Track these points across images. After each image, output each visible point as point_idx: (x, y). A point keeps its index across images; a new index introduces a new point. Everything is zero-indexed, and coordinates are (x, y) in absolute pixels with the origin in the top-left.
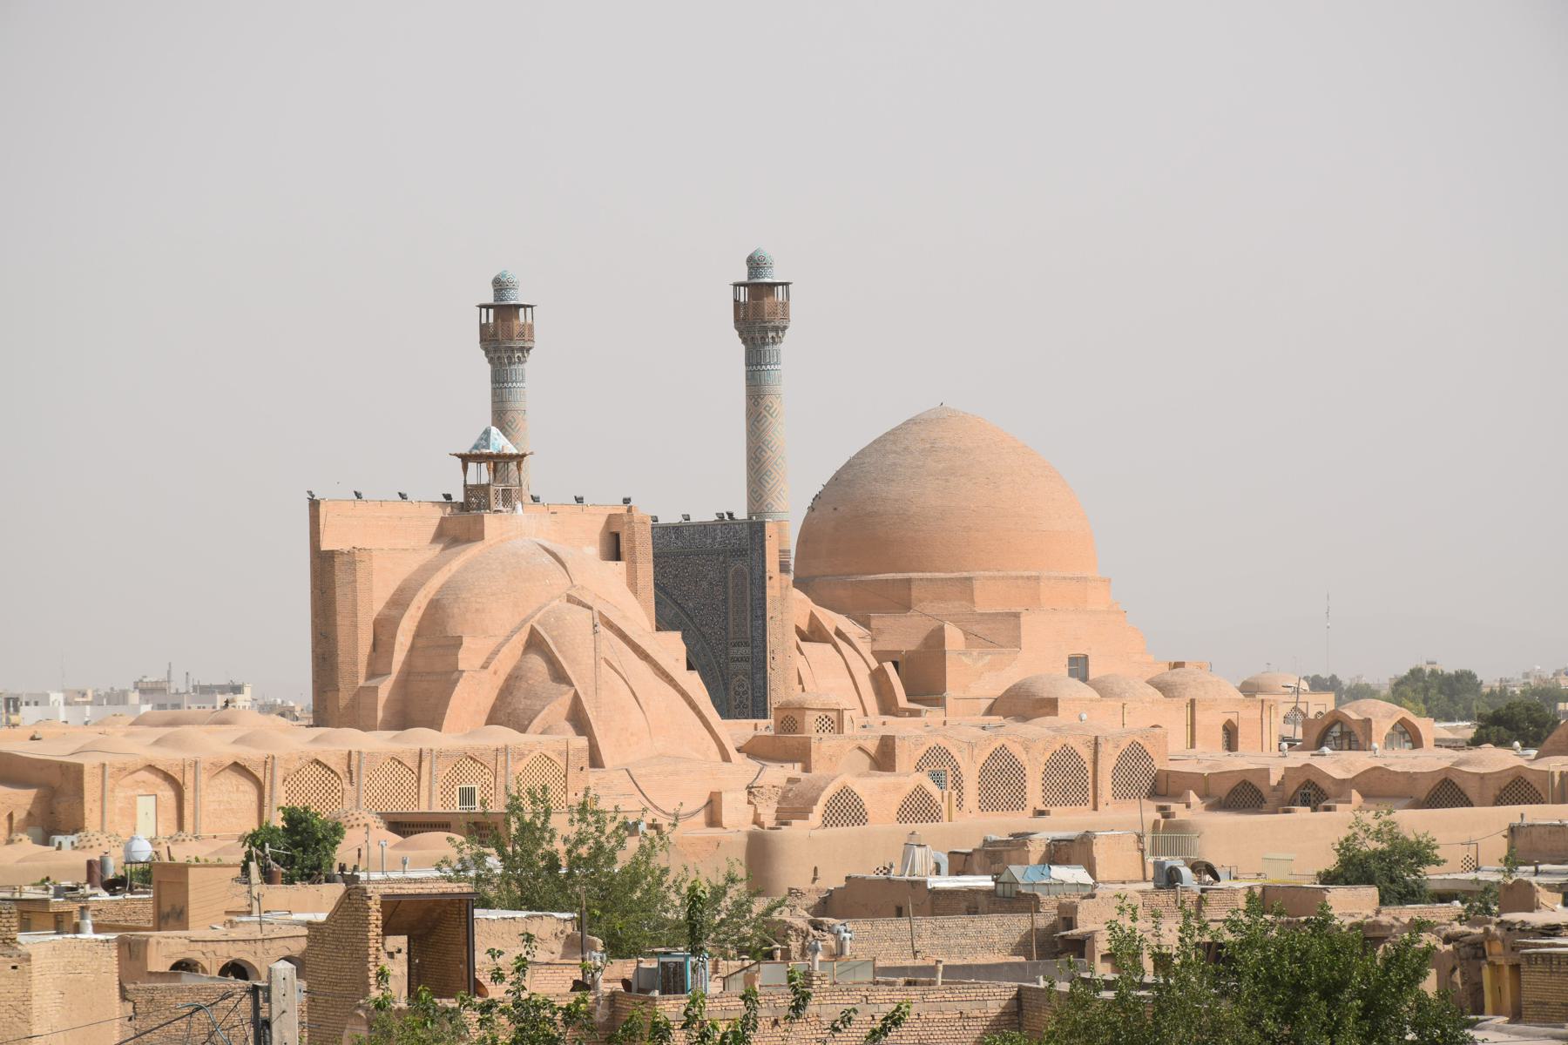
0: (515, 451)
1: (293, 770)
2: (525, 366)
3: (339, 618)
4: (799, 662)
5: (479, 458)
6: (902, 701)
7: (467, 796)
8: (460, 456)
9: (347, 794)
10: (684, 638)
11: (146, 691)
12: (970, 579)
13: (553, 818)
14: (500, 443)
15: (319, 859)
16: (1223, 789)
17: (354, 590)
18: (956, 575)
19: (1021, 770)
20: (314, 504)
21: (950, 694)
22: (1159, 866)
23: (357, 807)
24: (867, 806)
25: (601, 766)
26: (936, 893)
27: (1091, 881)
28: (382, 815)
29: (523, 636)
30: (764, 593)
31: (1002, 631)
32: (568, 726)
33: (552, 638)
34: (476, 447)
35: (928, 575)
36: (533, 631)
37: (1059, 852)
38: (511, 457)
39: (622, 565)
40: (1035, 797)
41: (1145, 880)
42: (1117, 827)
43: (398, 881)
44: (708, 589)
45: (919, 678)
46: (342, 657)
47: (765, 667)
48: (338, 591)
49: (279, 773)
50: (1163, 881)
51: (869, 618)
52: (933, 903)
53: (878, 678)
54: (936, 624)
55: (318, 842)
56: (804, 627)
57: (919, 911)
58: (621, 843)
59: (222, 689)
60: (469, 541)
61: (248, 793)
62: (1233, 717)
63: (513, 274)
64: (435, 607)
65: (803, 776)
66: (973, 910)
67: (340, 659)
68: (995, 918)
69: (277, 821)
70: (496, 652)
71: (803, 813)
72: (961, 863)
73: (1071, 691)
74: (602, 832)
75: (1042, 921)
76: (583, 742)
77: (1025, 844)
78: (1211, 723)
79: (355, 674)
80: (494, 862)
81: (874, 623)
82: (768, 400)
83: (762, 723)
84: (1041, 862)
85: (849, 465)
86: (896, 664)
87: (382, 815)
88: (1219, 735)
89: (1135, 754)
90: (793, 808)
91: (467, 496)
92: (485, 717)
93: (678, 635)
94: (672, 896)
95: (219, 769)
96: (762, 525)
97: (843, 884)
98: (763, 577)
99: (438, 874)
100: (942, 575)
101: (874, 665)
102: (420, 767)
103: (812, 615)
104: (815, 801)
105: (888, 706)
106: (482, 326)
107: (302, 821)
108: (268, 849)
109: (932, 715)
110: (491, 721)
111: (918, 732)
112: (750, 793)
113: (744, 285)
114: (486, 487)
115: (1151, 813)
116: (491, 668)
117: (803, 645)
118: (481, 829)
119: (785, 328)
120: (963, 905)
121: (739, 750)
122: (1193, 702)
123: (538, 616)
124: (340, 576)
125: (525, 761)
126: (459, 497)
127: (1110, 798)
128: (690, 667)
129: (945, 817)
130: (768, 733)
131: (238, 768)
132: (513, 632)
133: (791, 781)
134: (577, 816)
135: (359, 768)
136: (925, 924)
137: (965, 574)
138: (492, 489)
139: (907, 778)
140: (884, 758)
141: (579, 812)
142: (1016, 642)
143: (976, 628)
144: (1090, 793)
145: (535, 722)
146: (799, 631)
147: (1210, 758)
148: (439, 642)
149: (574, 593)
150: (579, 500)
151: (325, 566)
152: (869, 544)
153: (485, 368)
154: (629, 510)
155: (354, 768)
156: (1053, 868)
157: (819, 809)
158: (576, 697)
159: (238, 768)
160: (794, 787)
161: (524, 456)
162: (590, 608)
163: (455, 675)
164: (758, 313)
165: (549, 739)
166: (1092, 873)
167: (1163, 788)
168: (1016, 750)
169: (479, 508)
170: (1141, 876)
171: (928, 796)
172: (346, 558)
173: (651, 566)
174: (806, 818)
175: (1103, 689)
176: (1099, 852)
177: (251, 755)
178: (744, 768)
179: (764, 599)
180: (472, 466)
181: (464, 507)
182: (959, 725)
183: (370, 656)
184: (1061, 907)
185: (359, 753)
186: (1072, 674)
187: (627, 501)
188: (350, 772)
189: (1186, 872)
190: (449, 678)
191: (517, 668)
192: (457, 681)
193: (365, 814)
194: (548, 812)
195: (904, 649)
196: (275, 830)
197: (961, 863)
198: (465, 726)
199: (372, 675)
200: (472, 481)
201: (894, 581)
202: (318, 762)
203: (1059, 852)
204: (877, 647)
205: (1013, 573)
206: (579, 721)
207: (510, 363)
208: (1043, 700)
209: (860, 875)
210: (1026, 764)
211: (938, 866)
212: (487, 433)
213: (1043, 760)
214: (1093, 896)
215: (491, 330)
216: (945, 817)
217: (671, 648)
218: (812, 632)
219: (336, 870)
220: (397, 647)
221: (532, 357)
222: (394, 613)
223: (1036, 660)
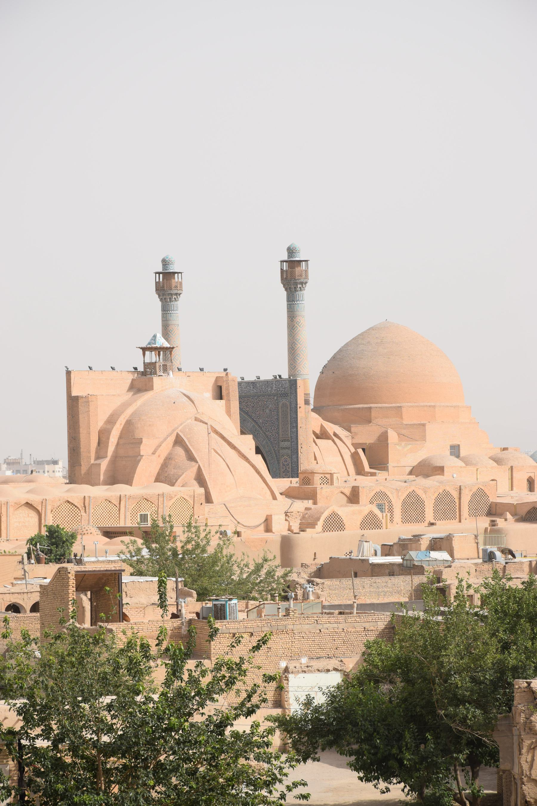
0: (168, 346)
1: (56, 506)
2: (178, 302)
3: (81, 430)
4: (315, 449)
5: (151, 349)
6: (367, 468)
7: (144, 518)
8: (141, 348)
9: (83, 517)
10: (253, 438)
11: (10, 463)
12: (400, 407)
13: (174, 530)
14: (161, 342)
15: (65, 552)
16: (523, 511)
17: (89, 416)
18: (394, 405)
19: (422, 502)
20: (68, 373)
21: (391, 465)
22: (485, 551)
23: (89, 524)
24: (344, 522)
25: (212, 502)
26: (374, 565)
27: (450, 559)
28: (99, 528)
29: (172, 438)
30: (297, 415)
31: (417, 433)
32: (195, 483)
33: (188, 439)
34: (149, 344)
35: (380, 405)
36: (178, 436)
37: (436, 545)
38: (167, 348)
39: (223, 402)
40: (429, 516)
41: (478, 557)
42: (467, 531)
43: (103, 562)
44: (268, 415)
45: (375, 457)
46: (83, 449)
47: (297, 452)
48: (81, 416)
49: (49, 508)
50: (487, 559)
51: (350, 427)
52: (372, 570)
53: (355, 457)
54: (383, 430)
55: (64, 542)
56: (318, 432)
57: (365, 574)
58: (208, 542)
59: (48, 462)
60: (146, 390)
61: (33, 517)
62: (532, 475)
63: (172, 256)
64: (129, 423)
65: (313, 507)
66: (392, 574)
67: (82, 450)
68: (402, 578)
69: (44, 533)
70: (159, 446)
71: (313, 525)
72: (387, 550)
73: (451, 463)
74: (199, 537)
75: (423, 579)
76: (202, 490)
77: (419, 540)
78: (521, 478)
79: (89, 458)
80: (145, 552)
81: (353, 429)
82: (298, 319)
83: (295, 480)
84: (426, 550)
85: (340, 351)
86: (364, 450)
87: (99, 528)
88: (525, 484)
89: (480, 494)
90: (307, 523)
91: (145, 368)
92: (154, 479)
93: (250, 437)
94: (237, 569)
95: (18, 506)
96: (295, 381)
97: (328, 561)
98: (297, 407)
99: (118, 558)
100: (386, 405)
101: (353, 450)
102: (120, 504)
103: (322, 426)
104: (318, 519)
105: (360, 471)
106: (156, 282)
107: (56, 532)
108: (38, 546)
109: (381, 475)
110: (157, 480)
111: (371, 484)
112: (286, 515)
113: (286, 261)
114: (156, 362)
115: (484, 522)
116: (157, 454)
117: (318, 441)
118: (150, 535)
119: (306, 283)
120: (387, 571)
121: (281, 494)
122: (512, 467)
123: (180, 428)
124: (82, 408)
125: (173, 500)
126: (141, 369)
127: (468, 516)
128: (258, 451)
129: (384, 527)
130: (298, 485)
131: (28, 505)
132: (168, 436)
133: (306, 509)
134: (186, 529)
135: (89, 504)
136: (367, 581)
137: (398, 405)
138: (157, 365)
139: (365, 507)
140: (354, 497)
141: (187, 527)
142: (423, 438)
143: (404, 432)
144: (458, 514)
145: (179, 481)
146: (314, 433)
147: (521, 496)
148: (131, 440)
149: (199, 417)
150: (202, 370)
151: (74, 404)
152: (347, 390)
153: (158, 304)
154: (227, 374)
155: (87, 505)
156: (431, 552)
157: (320, 523)
158: (199, 467)
159: (28, 505)
160: (308, 512)
161: (173, 348)
162: (206, 424)
163: (139, 457)
164: (292, 275)
165: (187, 489)
166: (452, 555)
167: (494, 511)
168: (420, 493)
169: (151, 374)
170: (476, 556)
171: (375, 516)
172: (84, 400)
173: (238, 402)
174: (314, 528)
175: (467, 462)
176: (456, 544)
177: (34, 499)
178: (284, 502)
179: (297, 418)
180: (147, 353)
181: (144, 374)
182: (394, 482)
183: (97, 448)
184: (435, 572)
185: (89, 497)
186: (451, 454)
187: (225, 370)
188: (85, 507)
189: (498, 554)
190: (136, 459)
191: (170, 454)
192: (140, 461)
193: (91, 527)
194: (172, 527)
195: (368, 442)
196: (42, 537)
197: (387, 550)
198: (144, 483)
199: (98, 457)
200: (147, 360)
201: (363, 408)
202: (68, 502)
203: (436, 545)
204: (356, 441)
205: (422, 404)
206: (201, 480)
207: (170, 301)
208: (437, 467)
209: (336, 556)
210: (425, 500)
211: (376, 551)
212: (155, 336)
213: (434, 497)
214: (450, 566)
215: (161, 285)
216: (384, 527)
217: (247, 444)
218: (322, 434)
219: (72, 557)
220: (110, 444)
221: (181, 298)
222: (109, 426)
223: (434, 448)
